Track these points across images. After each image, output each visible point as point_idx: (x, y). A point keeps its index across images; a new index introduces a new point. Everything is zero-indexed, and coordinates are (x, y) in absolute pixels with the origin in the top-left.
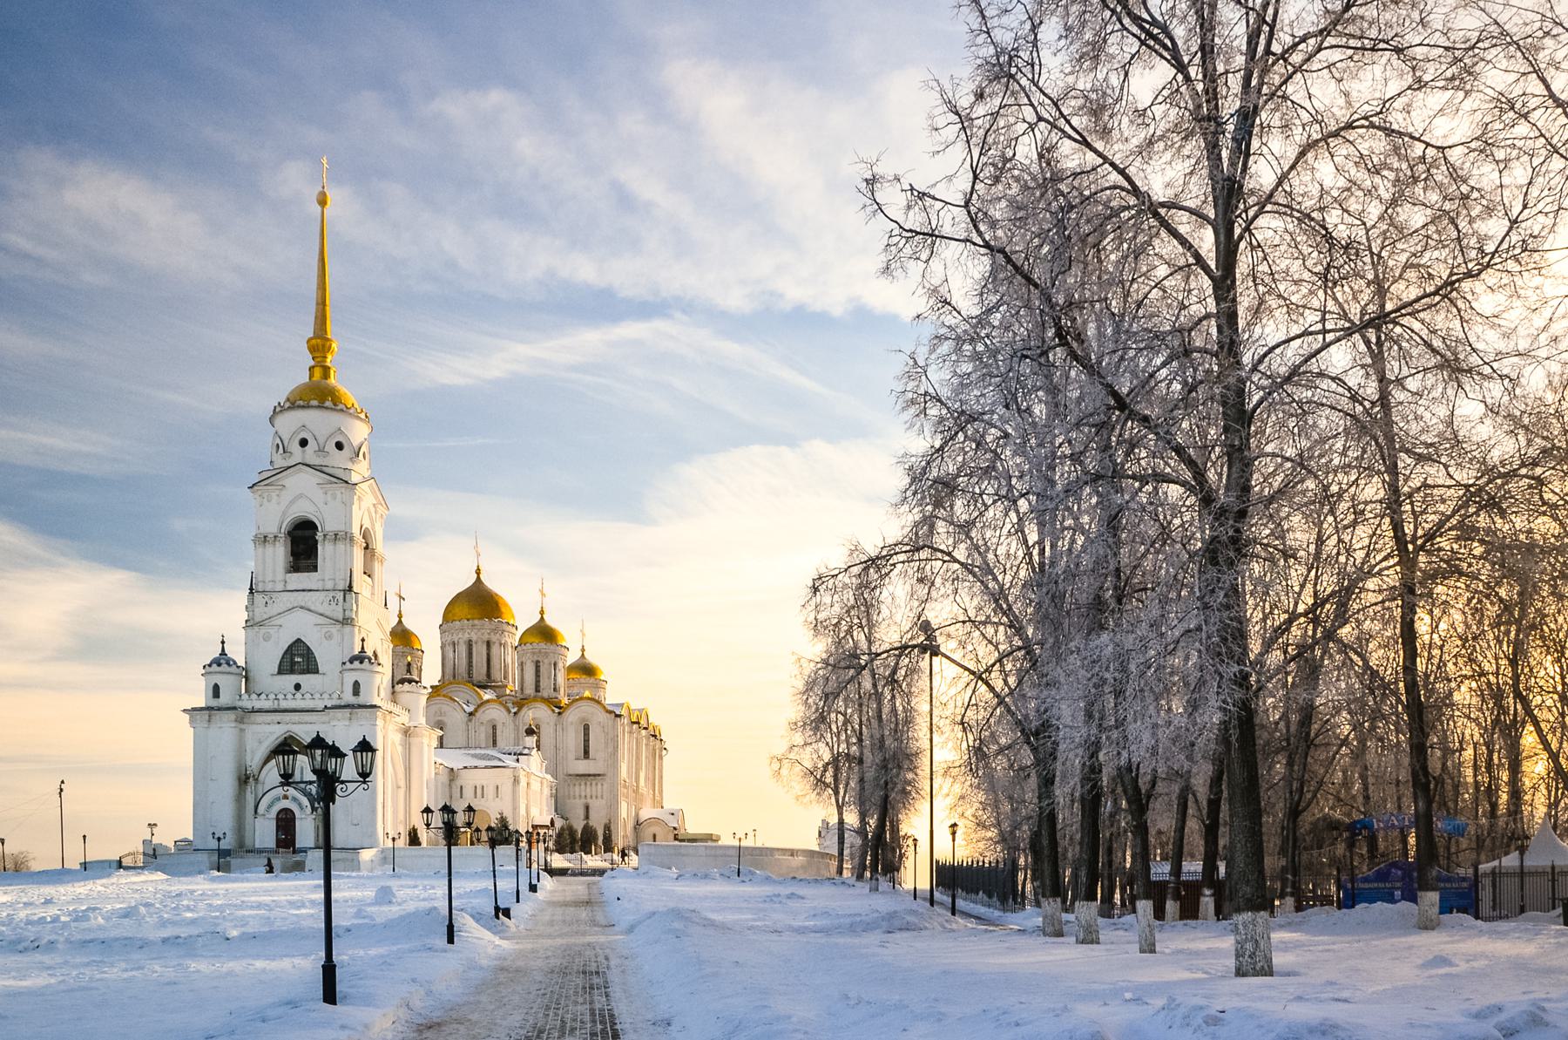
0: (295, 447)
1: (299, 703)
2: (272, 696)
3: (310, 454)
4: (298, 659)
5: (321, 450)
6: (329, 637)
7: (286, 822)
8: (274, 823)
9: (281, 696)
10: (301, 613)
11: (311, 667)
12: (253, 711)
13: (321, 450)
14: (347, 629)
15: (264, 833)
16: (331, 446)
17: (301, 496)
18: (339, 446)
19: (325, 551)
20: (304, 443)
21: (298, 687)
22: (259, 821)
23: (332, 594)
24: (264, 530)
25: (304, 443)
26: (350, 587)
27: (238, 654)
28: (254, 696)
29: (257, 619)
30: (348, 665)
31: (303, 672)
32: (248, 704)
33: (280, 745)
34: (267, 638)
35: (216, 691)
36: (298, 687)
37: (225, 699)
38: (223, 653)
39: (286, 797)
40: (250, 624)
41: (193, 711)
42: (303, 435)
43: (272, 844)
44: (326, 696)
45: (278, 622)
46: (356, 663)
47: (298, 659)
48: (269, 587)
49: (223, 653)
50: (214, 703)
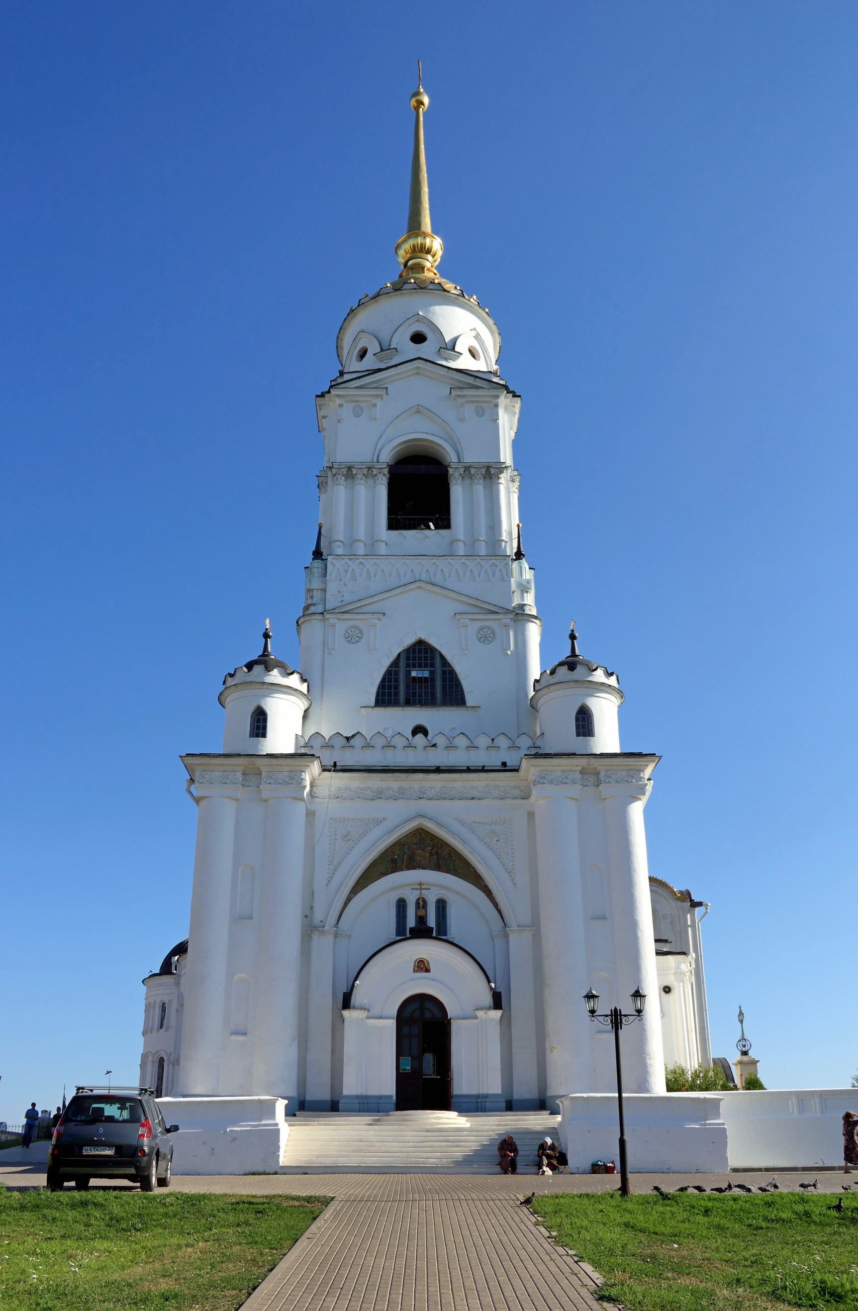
2: (379, 742)
8: (392, 1024)
9: (399, 742)
15: (372, 1056)
17: (418, 410)
18: (473, 353)
25: (418, 338)
33: (399, 844)
34: (354, 637)
39: (422, 966)
44: (502, 742)
45: (376, 607)
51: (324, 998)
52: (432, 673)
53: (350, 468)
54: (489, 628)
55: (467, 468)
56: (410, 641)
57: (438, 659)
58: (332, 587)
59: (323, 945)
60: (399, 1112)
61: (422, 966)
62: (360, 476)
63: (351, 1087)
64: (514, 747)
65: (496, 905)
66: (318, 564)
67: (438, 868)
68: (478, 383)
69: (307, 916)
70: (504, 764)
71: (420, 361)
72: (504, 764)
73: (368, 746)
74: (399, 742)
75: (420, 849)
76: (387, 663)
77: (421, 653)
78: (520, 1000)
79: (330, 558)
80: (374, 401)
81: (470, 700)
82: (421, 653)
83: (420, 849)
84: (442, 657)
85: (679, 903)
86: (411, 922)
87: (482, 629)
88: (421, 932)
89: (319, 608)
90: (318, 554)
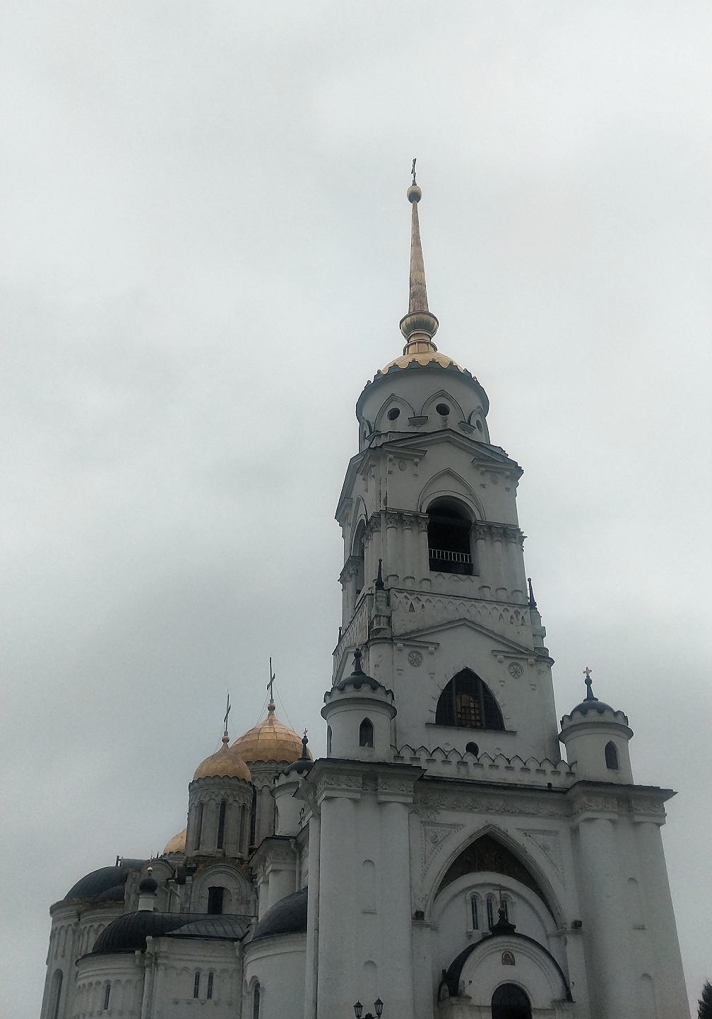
2: (454, 759)
6: (516, 674)
10: (465, 634)
11: (491, 719)
14: (543, 666)
17: (449, 473)
19: (484, 551)
20: (443, 410)
21: (472, 748)
23: (512, 611)
31: (475, 727)
34: (415, 662)
37: (381, 751)
38: (358, 671)
47: (467, 703)
48: (409, 585)
50: (363, 754)
54: (518, 664)
57: (481, 686)
61: (508, 960)
65: (548, 907)
66: (380, 593)
67: (501, 870)
70: (550, 785)
72: (550, 785)
73: (446, 762)
75: (490, 852)
77: (466, 683)
80: (417, 460)
81: (508, 725)
82: (466, 683)
83: (490, 852)
84: (484, 685)
87: (511, 665)
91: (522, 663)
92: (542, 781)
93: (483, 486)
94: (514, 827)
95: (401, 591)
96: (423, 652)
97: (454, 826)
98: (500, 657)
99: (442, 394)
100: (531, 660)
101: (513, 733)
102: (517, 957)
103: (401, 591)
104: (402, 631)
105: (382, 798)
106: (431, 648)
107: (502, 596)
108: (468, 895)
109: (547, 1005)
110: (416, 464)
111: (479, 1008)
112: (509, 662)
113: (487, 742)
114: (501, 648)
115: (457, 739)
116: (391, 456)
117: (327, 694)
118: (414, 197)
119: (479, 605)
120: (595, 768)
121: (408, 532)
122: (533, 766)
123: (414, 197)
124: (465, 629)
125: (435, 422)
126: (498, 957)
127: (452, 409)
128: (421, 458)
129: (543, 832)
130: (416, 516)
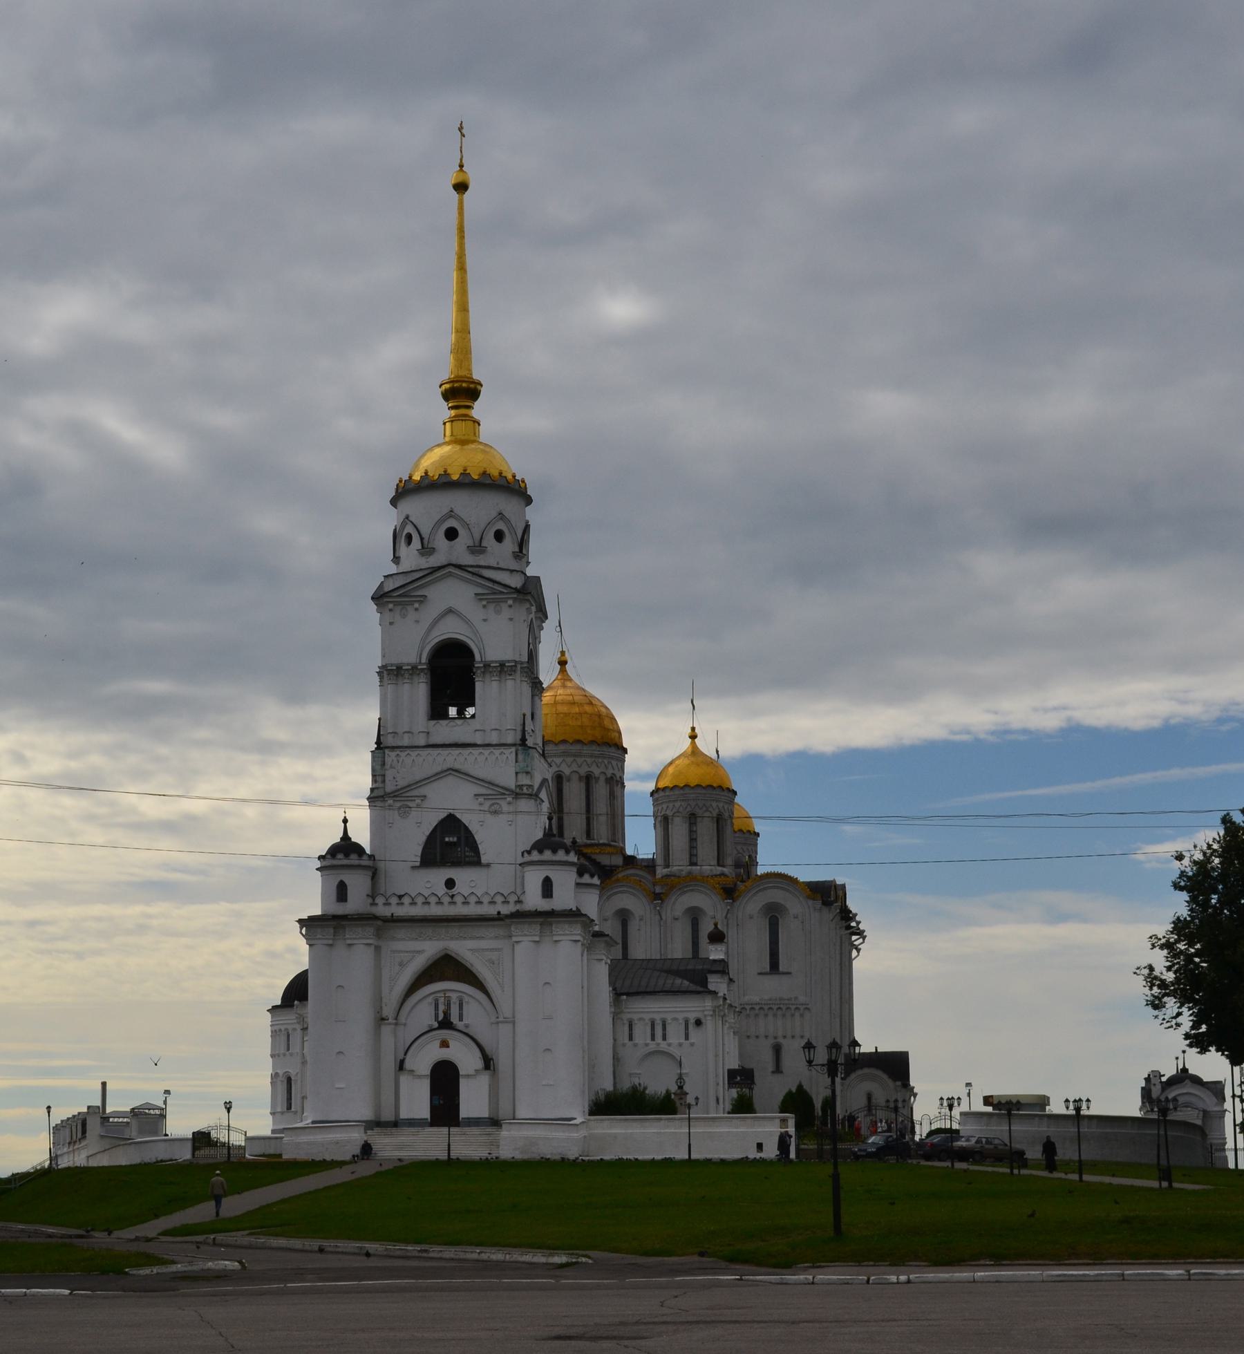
0: (440, 541)
1: (460, 910)
2: (420, 900)
3: (459, 551)
4: (451, 845)
5: (477, 548)
7: (445, 1080)
9: (433, 900)
10: (451, 780)
12: (393, 920)
13: (477, 548)
15: (416, 1100)
16: (490, 541)
17: (450, 611)
18: (499, 536)
19: (485, 689)
20: (451, 534)
21: (450, 884)
22: (404, 1079)
24: (395, 660)
25: (451, 534)
26: (523, 740)
27: (362, 835)
28: (394, 900)
29: (390, 787)
30: (535, 856)
31: (458, 863)
32: (381, 910)
35: (342, 892)
36: (450, 884)
37: (357, 902)
38: (346, 837)
39: (445, 1044)
40: (376, 798)
41: (309, 924)
42: (452, 523)
43: (424, 1113)
44: (499, 899)
46: (548, 855)
47: (451, 845)
48: (406, 741)
49: (346, 837)
50: (340, 909)
51: (389, 1064)
52: (459, 838)
53: (399, 668)
55: (487, 666)
56: (443, 815)
58: (389, 775)
59: (386, 1030)
60: (435, 1129)
61: (445, 1044)
62: (407, 676)
63: (404, 1114)
64: (506, 902)
67: (458, 979)
68: (496, 587)
69: (379, 1010)
71: (451, 569)
73: (413, 903)
74: (433, 900)
75: (447, 968)
76: (428, 833)
77: (451, 824)
78: (503, 1062)
79: (387, 751)
80: (416, 605)
81: (484, 860)
82: (451, 824)
84: (466, 828)
85: (810, 902)
86: (441, 1017)
88: (446, 1024)
89: (380, 793)
90: (378, 742)
91: (503, 804)
92: (491, 911)
93: (485, 620)
94: (465, 948)
95: (393, 748)
96: (410, 804)
97: (419, 952)
98: (481, 799)
99: (451, 514)
100: (509, 799)
101: (488, 865)
102: (451, 1043)
103: (393, 748)
104: (394, 788)
105: (349, 942)
106: (418, 801)
107: (494, 739)
108: (430, 999)
109: (472, 1072)
110: (416, 609)
111: (420, 1077)
112: (488, 803)
113: (465, 878)
114: (483, 791)
115: (436, 878)
116: (391, 606)
117: (320, 858)
118: (461, 187)
119: (466, 751)
120: (534, 900)
121: (407, 686)
122: (486, 900)
123: (461, 187)
124: (451, 777)
125: (444, 551)
126: (437, 1043)
127: (461, 532)
128: (421, 602)
129: (492, 950)
130: (414, 669)
